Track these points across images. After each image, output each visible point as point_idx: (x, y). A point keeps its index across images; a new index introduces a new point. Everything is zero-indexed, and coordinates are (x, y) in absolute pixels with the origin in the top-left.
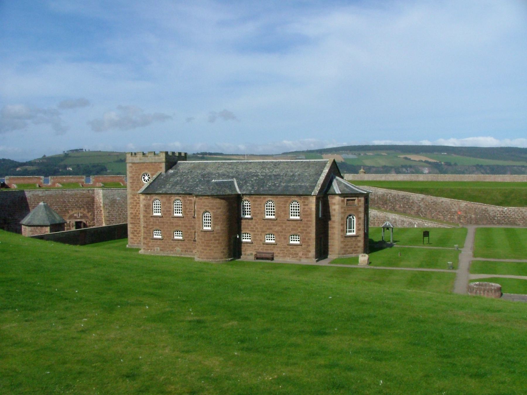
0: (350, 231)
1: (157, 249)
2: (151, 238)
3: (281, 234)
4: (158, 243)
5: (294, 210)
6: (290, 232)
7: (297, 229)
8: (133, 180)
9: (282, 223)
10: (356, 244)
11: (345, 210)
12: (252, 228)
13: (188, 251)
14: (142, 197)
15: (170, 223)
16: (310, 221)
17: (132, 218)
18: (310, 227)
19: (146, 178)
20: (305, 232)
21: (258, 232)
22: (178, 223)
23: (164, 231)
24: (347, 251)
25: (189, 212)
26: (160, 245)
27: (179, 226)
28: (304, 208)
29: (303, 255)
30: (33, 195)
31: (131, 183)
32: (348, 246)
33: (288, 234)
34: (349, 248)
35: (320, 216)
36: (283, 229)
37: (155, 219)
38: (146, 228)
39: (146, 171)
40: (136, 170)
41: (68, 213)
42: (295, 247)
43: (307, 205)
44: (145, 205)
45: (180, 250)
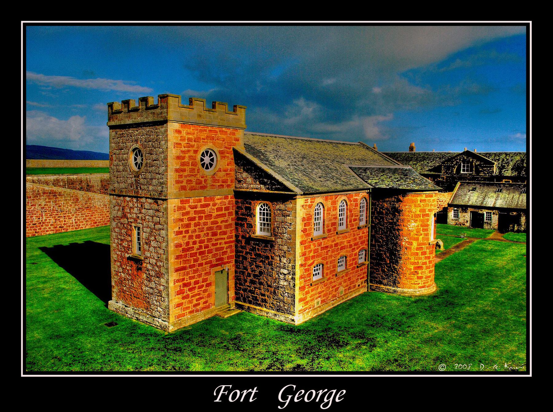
8: (183, 164)
15: (336, 245)
17: (178, 257)
19: (207, 160)
31: (177, 171)
40: (189, 140)
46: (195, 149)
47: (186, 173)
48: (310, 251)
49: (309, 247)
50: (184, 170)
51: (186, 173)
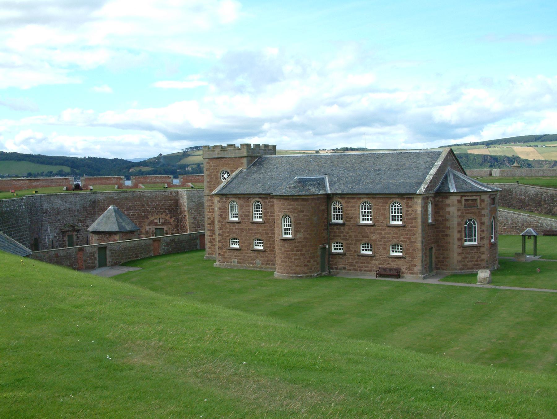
0: (470, 240)
1: (234, 262)
2: (228, 247)
3: (379, 243)
4: (235, 254)
5: (365, 212)
6: (390, 241)
7: (399, 238)
8: (211, 179)
9: (381, 230)
10: (479, 257)
11: (462, 213)
12: (344, 236)
13: (269, 264)
14: (216, 199)
15: (249, 229)
16: (415, 227)
18: (414, 234)
20: (408, 241)
21: (352, 241)
22: (258, 230)
23: (242, 239)
24: (467, 265)
25: (270, 216)
26: (238, 256)
27: (259, 233)
28: (407, 211)
29: (406, 270)
30: (107, 198)
31: (208, 182)
32: (468, 260)
33: (388, 244)
34: (468, 262)
35: (430, 221)
36: (382, 238)
37: (231, 224)
38: (222, 235)
39: (225, 168)
41: (148, 218)
42: (397, 260)
43: (411, 207)
44: (220, 209)
45: (261, 262)
46: (217, 170)
47: (213, 183)
48: (227, 228)
49: (225, 225)
50: (212, 182)
51: (213, 183)
